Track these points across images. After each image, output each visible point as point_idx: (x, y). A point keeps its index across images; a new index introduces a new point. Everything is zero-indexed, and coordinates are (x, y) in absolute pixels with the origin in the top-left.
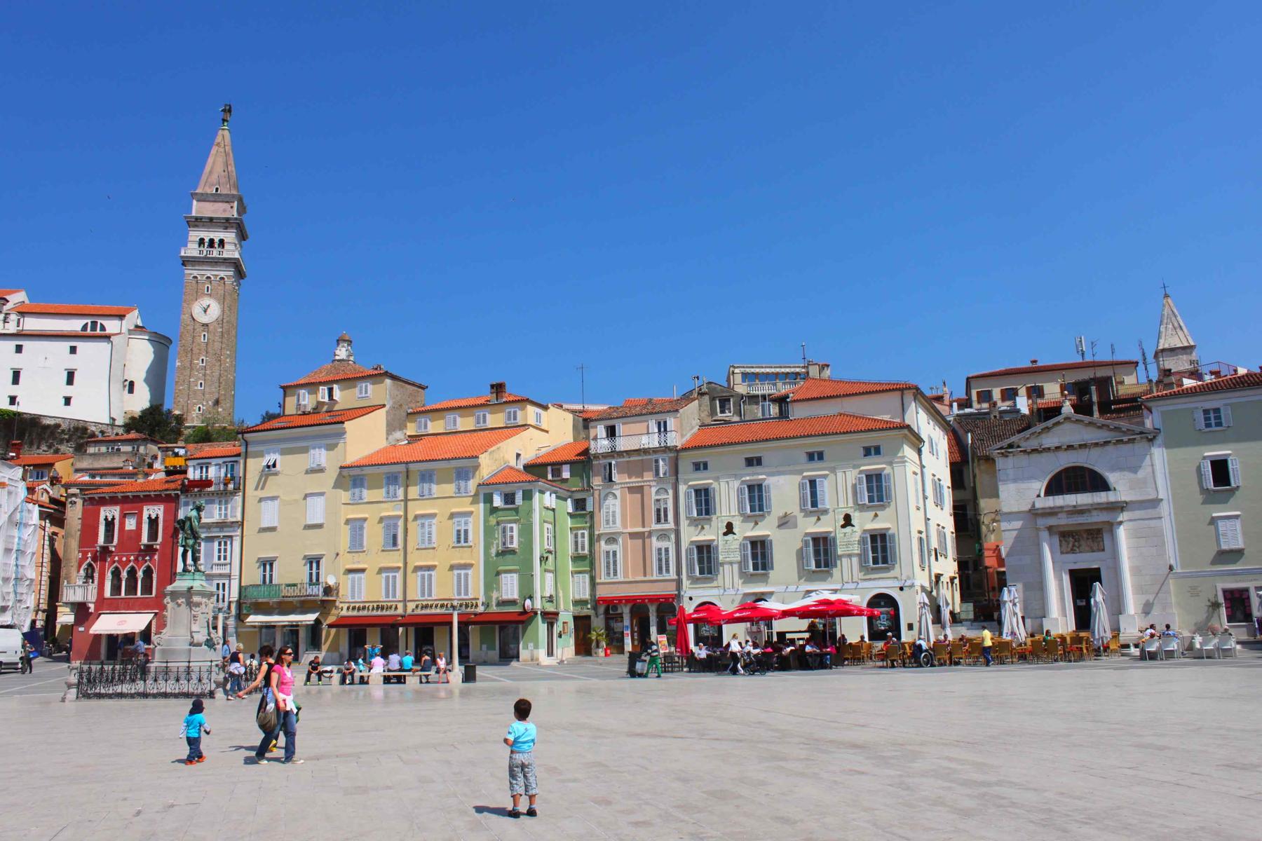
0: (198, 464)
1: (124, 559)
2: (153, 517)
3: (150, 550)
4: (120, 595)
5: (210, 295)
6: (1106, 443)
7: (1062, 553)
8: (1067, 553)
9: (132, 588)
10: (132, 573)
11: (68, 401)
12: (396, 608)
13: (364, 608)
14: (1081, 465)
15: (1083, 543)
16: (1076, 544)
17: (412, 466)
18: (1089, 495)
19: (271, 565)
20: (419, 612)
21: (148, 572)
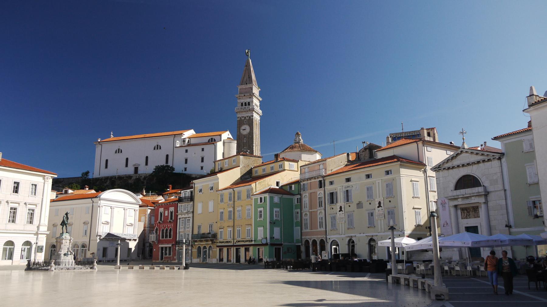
0: (184, 192)
1: (165, 226)
2: (172, 211)
3: (170, 222)
4: (164, 238)
5: (246, 124)
6: (478, 162)
7: (462, 218)
8: (464, 218)
9: (166, 237)
10: (167, 230)
11: (202, 168)
12: (231, 242)
13: (223, 242)
14: (469, 174)
15: (471, 213)
16: (468, 214)
17: (234, 189)
18: (471, 189)
19: (200, 227)
20: (237, 244)
21: (170, 230)
